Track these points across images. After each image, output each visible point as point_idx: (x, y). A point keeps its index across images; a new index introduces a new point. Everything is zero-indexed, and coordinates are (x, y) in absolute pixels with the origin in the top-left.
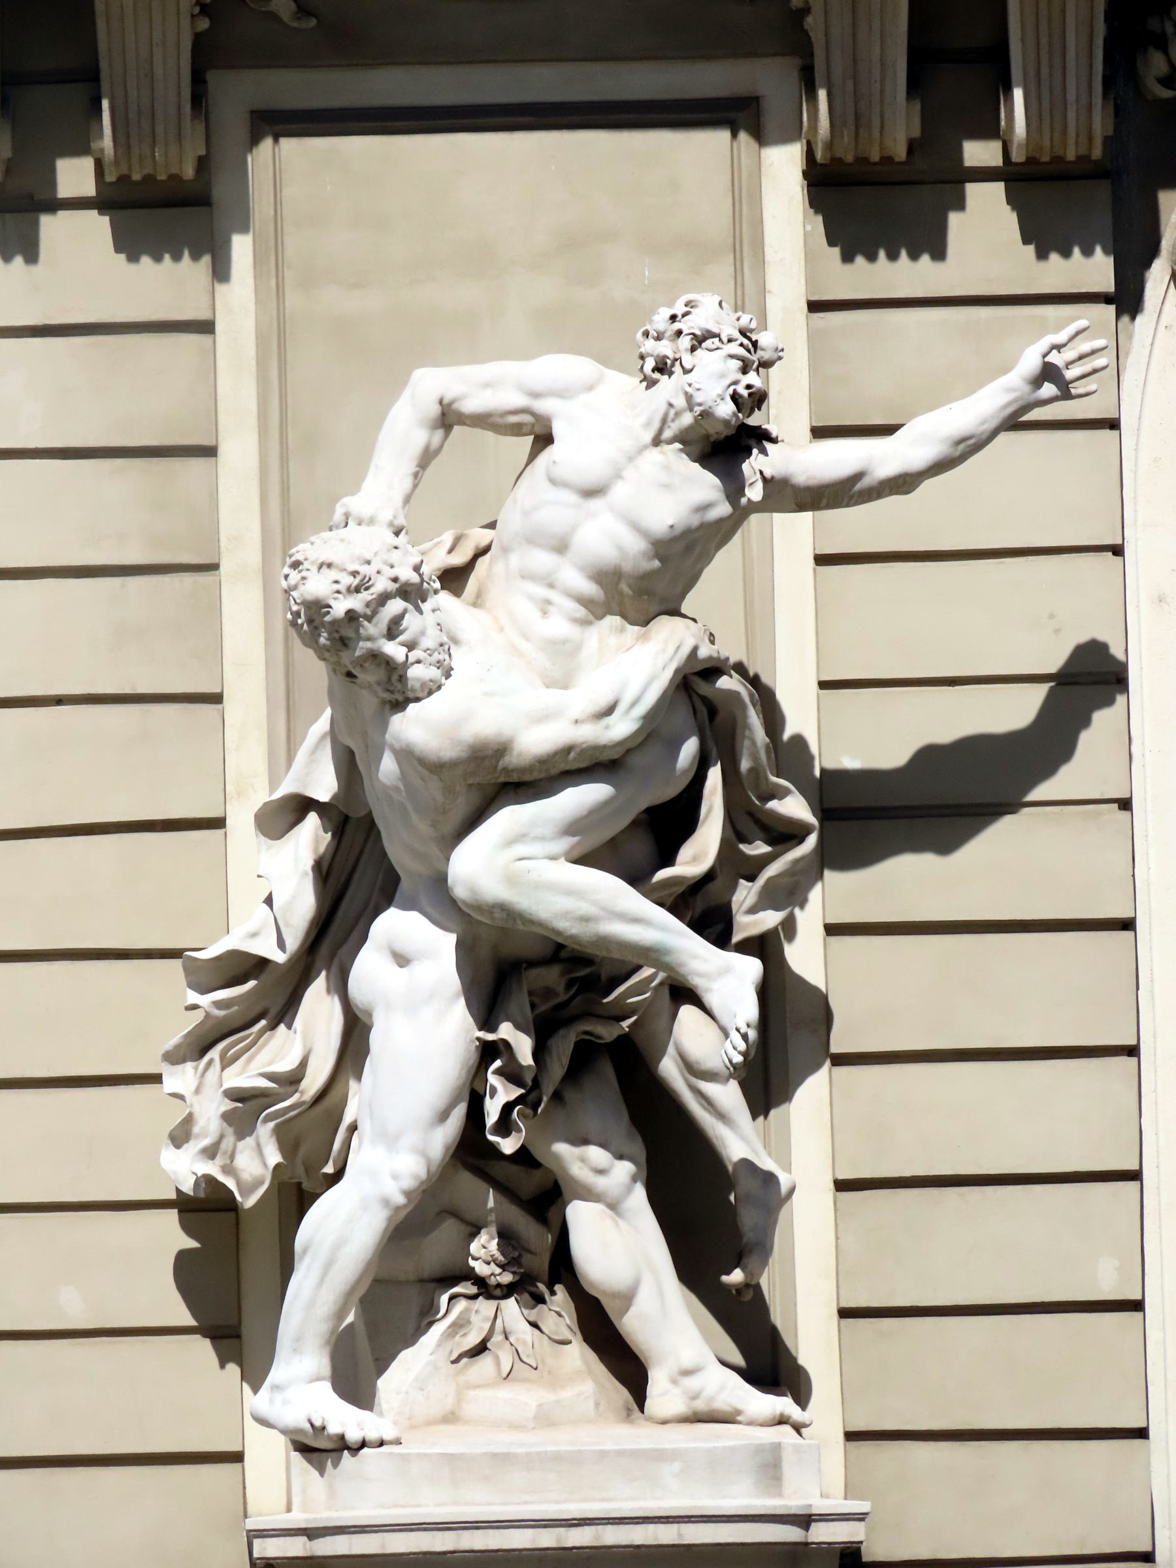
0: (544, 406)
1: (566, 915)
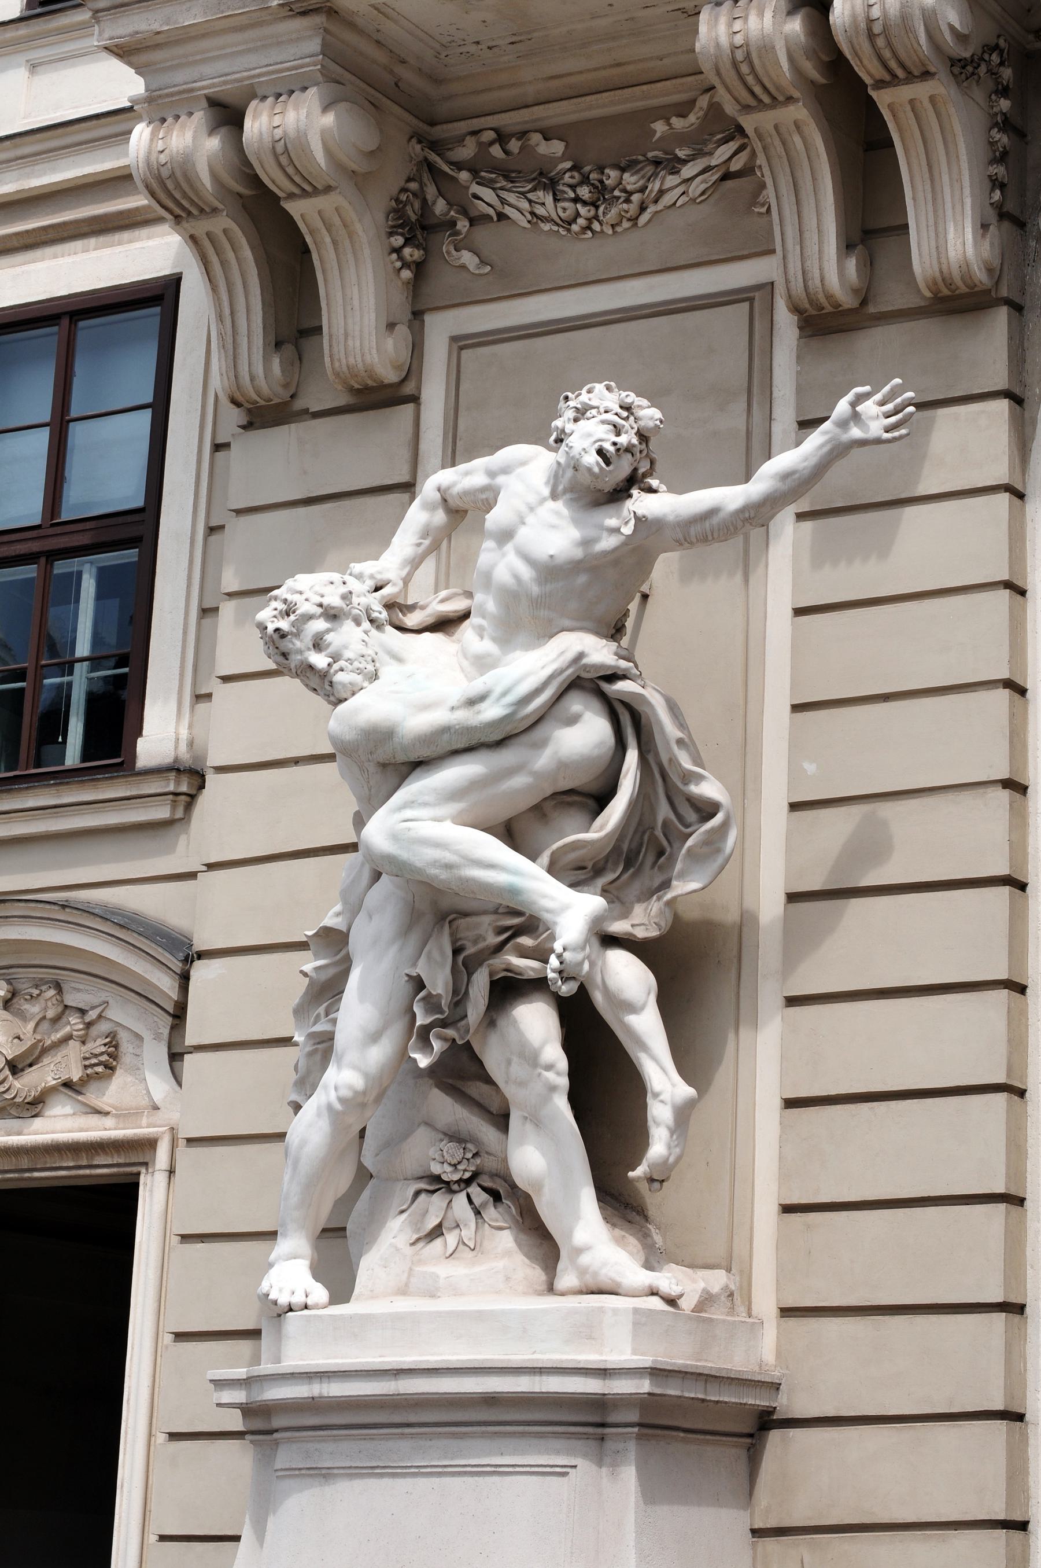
1: (435, 863)
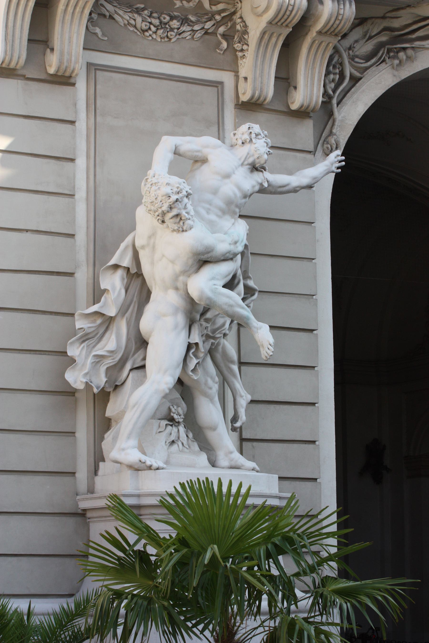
0: (206, 151)
1: (226, 304)
